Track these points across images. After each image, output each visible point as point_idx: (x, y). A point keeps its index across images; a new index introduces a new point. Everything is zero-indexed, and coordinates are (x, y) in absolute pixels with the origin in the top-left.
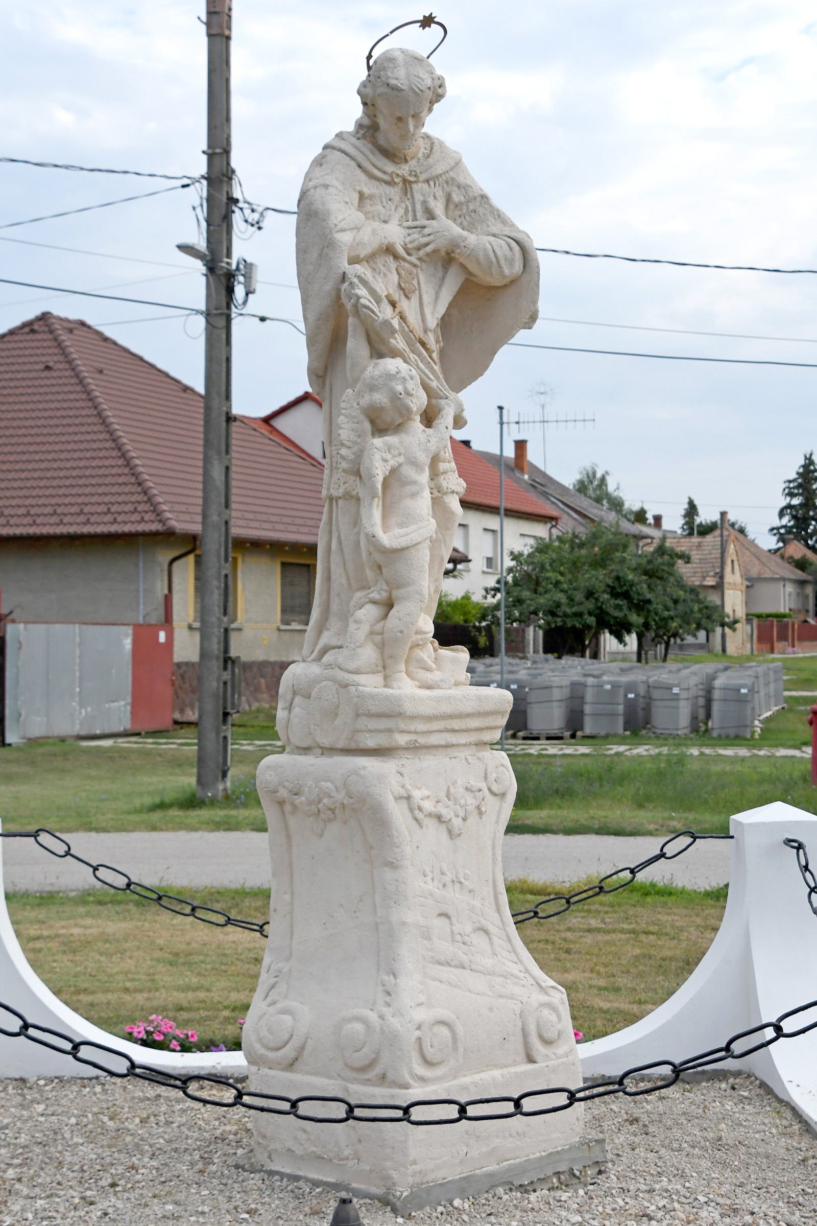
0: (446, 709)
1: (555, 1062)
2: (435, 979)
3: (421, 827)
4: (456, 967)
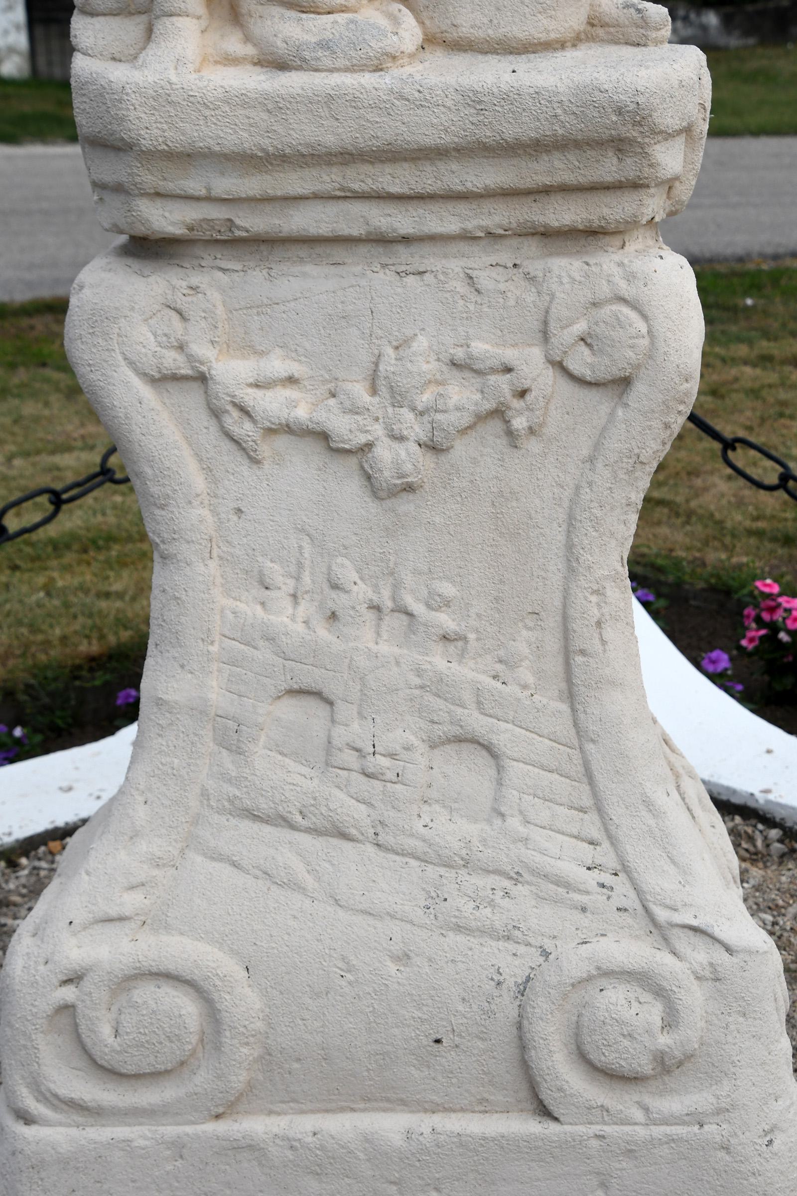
0: (304, 132)
1: (641, 1132)
2: (217, 857)
3: (255, 461)
4: (308, 830)
